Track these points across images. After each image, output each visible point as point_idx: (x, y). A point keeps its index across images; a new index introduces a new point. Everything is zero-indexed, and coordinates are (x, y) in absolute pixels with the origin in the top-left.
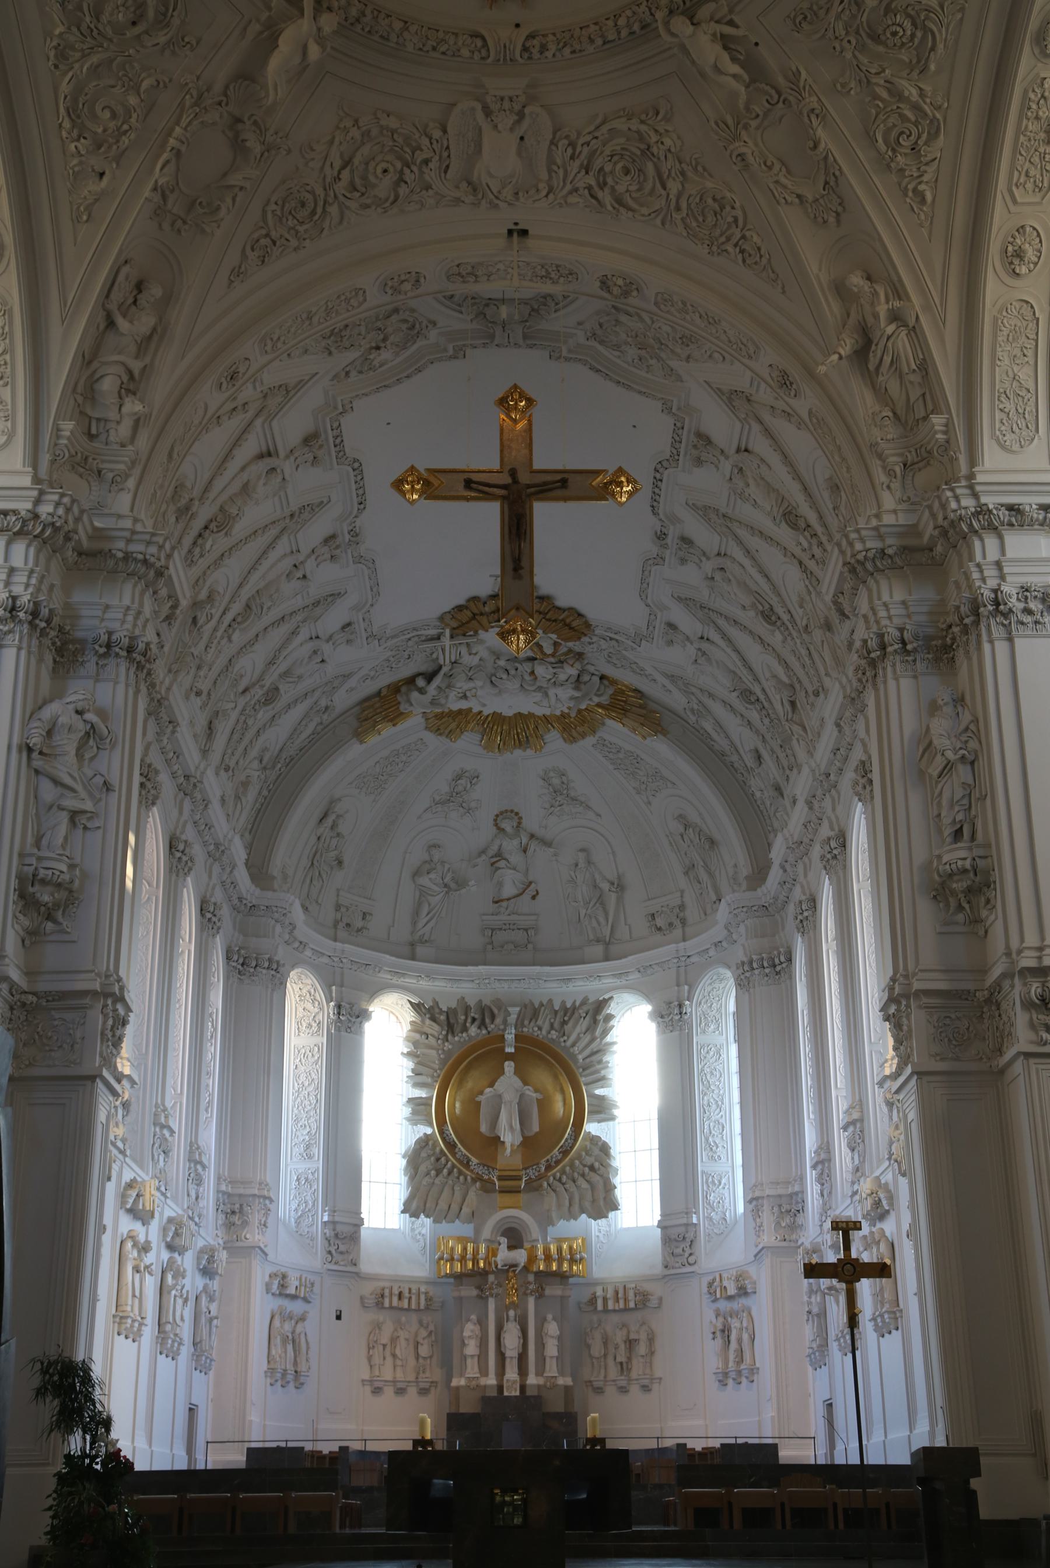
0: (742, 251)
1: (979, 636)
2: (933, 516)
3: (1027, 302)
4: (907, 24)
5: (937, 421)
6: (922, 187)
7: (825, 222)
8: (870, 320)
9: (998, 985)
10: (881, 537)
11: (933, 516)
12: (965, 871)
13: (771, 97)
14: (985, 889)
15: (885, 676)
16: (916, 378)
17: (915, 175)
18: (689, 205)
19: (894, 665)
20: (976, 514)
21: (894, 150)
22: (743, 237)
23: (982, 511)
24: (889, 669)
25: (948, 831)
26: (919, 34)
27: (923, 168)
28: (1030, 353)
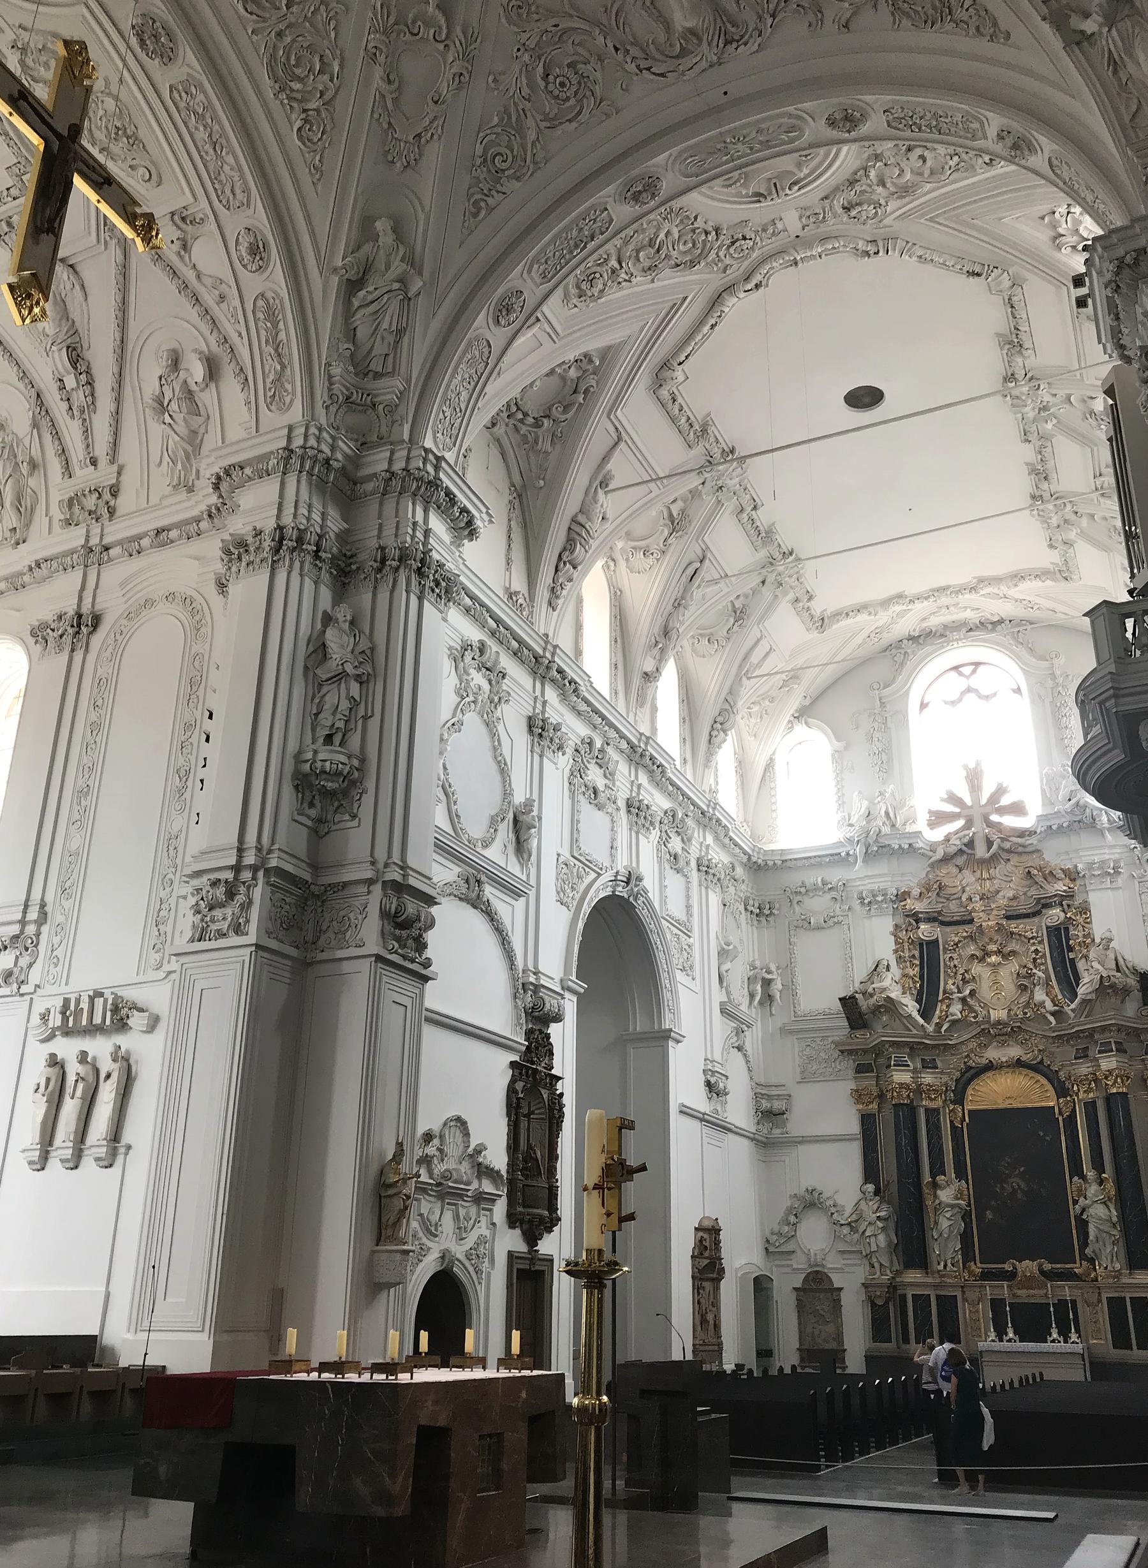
0: (306, 121)
1: (395, 581)
2: (391, 461)
3: (490, 346)
4: (574, 89)
5: (398, 383)
6: (483, 204)
7: (393, 162)
8: (380, 264)
9: (345, 885)
10: (333, 448)
11: (391, 461)
12: (341, 773)
13: (440, 33)
14: (340, 796)
15: (291, 566)
16: (391, 339)
17: (485, 192)
18: (294, 41)
19: (302, 563)
20: (430, 482)
21: (485, 160)
22: (317, 110)
23: (435, 484)
24: (297, 564)
25: (322, 733)
26: (572, 102)
27: (494, 193)
28: (473, 384)
